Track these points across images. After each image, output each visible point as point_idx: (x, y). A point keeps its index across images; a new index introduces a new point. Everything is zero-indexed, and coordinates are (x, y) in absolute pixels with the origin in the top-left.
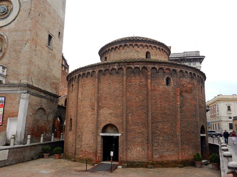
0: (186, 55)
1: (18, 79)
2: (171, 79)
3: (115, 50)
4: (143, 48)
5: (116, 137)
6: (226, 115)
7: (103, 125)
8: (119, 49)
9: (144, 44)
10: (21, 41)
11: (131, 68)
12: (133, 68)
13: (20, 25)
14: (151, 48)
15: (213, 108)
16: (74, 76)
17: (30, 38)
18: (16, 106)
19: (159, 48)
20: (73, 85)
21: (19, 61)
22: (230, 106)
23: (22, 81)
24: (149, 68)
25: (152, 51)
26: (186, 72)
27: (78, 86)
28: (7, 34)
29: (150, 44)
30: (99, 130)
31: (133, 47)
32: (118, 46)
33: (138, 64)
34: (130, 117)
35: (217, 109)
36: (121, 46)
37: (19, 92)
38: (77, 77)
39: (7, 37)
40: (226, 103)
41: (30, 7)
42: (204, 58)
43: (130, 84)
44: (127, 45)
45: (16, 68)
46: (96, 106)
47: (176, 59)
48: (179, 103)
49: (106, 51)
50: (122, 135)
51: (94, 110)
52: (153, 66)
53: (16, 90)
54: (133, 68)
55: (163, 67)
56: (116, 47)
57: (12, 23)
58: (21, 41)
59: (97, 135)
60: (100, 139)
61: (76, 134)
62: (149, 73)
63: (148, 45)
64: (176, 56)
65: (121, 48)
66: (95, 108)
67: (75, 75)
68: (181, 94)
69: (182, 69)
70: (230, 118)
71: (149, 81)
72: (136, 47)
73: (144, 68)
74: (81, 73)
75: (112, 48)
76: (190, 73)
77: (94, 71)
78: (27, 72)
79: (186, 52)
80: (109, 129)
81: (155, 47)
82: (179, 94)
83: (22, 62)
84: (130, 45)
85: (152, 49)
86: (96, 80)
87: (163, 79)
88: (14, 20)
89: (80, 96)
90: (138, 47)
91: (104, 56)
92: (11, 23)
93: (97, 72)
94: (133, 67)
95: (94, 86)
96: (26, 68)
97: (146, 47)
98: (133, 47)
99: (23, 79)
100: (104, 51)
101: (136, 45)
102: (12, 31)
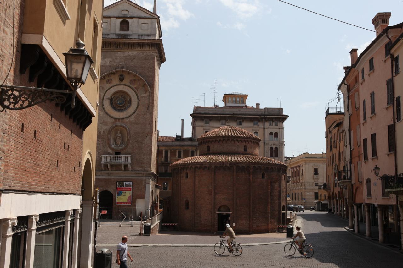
0: (268, 112)
1: (142, 167)
2: (265, 174)
3: (219, 142)
4: (242, 142)
6: (311, 181)
7: (219, 206)
8: (222, 142)
9: (243, 140)
10: (142, 133)
12: (241, 167)
14: (248, 142)
15: (297, 169)
16: (190, 166)
19: (254, 142)
20: (187, 174)
22: (317, 169)
23: (146, 169)
25: (248, 144)
26: (275, 168)
27: (195, 175)
28: (128, 126)
29: (247, 140)
30: (216, 210)
31: (235, 142)
32: (222, 140)
33: (244, 164)
34: (238, 201)
35: (301, 173)
36: (224, 140)
38: (194, 168)
40: (312, 164)
41: (148, 102)
42: (287, 118)
43: (238, 177)
44: (230, 140)
45: (139, 157)
46: (213, 192)
47: (256, 116)
48: (269, 191)
49: (209, 141)
50: (233, 213)
51: (211, 195)
52: (254, 165)
54: (241, 167)
55: (261, 165)
56: (220, 140)
57: (132, 116)
58: (142, 133)
59: (215, 213)
60: (216, 216)
61: (195, 213)
62: (251, 171)
63: (246, 140)
64: (256, 112)
65: (224, 142)
66: (212, 194)
67: (191, 166)
68: (271, 184)
69: (272, 166)
70: (316, 185)
71: (251, 176)
72: (236, 142)
73: (248, 167)
74: (198, 166)
75: (216, 140)
76: (278, 168)
77: (210, 166)
79: (267, 108)
80: (222, 209)
81: (251, 141)
82: (270, 184)
84: (232, 140)
85: (248, 143)
86: (213, 173)
87: (260, 175)
89: (197, 183)
90: (238, 142)
91: (206, 144)
93: (213, 167)
94: (241, 166)
95: (210, 177)
97: (244, 142)
98: (235, 142)
100: (208, 140)
101: (237, 140)
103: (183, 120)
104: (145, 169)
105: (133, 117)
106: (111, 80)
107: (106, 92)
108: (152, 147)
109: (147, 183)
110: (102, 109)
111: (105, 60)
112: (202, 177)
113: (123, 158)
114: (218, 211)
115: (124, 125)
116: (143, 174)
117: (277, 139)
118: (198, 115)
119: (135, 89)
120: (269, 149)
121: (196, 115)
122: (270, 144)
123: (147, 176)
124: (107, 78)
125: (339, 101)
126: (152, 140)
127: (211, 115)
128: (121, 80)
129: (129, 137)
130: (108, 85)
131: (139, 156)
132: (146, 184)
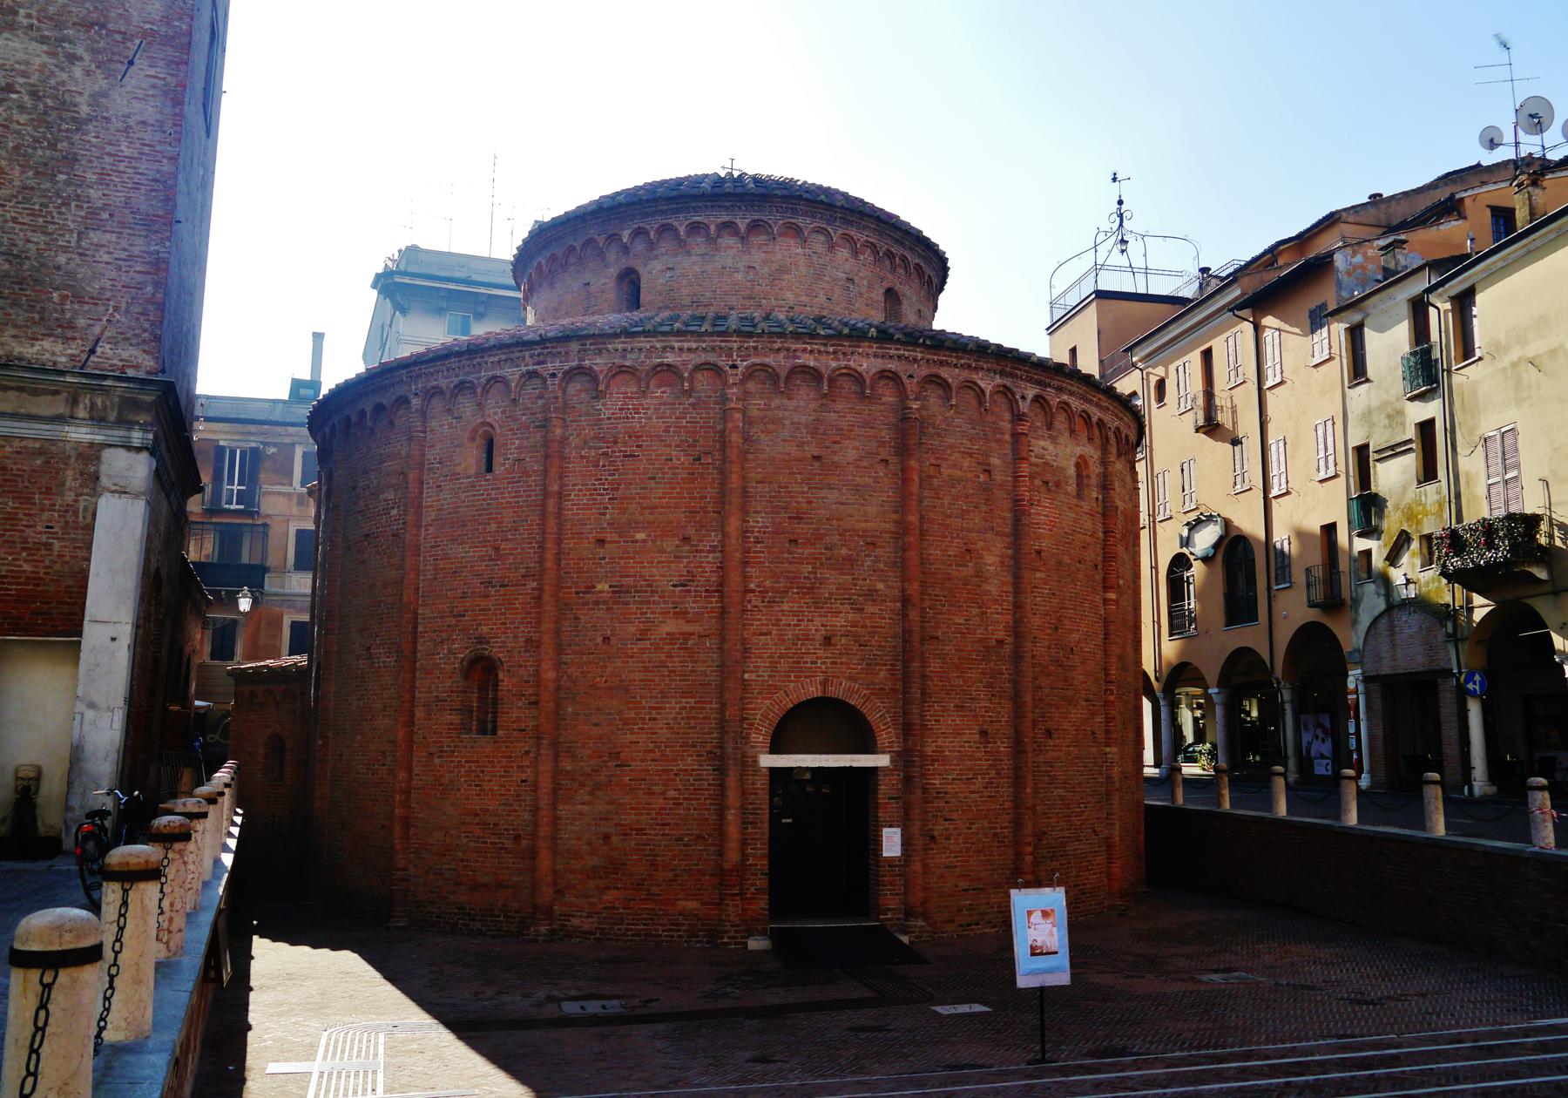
5: (808, 776)
10: (87, 25)
11: (944, 385)
17: (167, 20)
18: (57, 545)
21: (68, 183)
23: (104, 349)
24: (1023, 398)
32: (742, 225)
37: (80, 434)
58: (87, 25)
78: (149, 289)
83: (99, 204)
96: (136, 251)
99: (114, 342)
103: (318, 337)
104: (92, 351)
109: (105, 481)
112: (631, 456)
114: (775, 749)
116: (74, 401)
118: (418, 282)
121: (407, 280)
123: (112, 416)
125: (1123, 251)
127: (483, 290)
132: (95, 494)
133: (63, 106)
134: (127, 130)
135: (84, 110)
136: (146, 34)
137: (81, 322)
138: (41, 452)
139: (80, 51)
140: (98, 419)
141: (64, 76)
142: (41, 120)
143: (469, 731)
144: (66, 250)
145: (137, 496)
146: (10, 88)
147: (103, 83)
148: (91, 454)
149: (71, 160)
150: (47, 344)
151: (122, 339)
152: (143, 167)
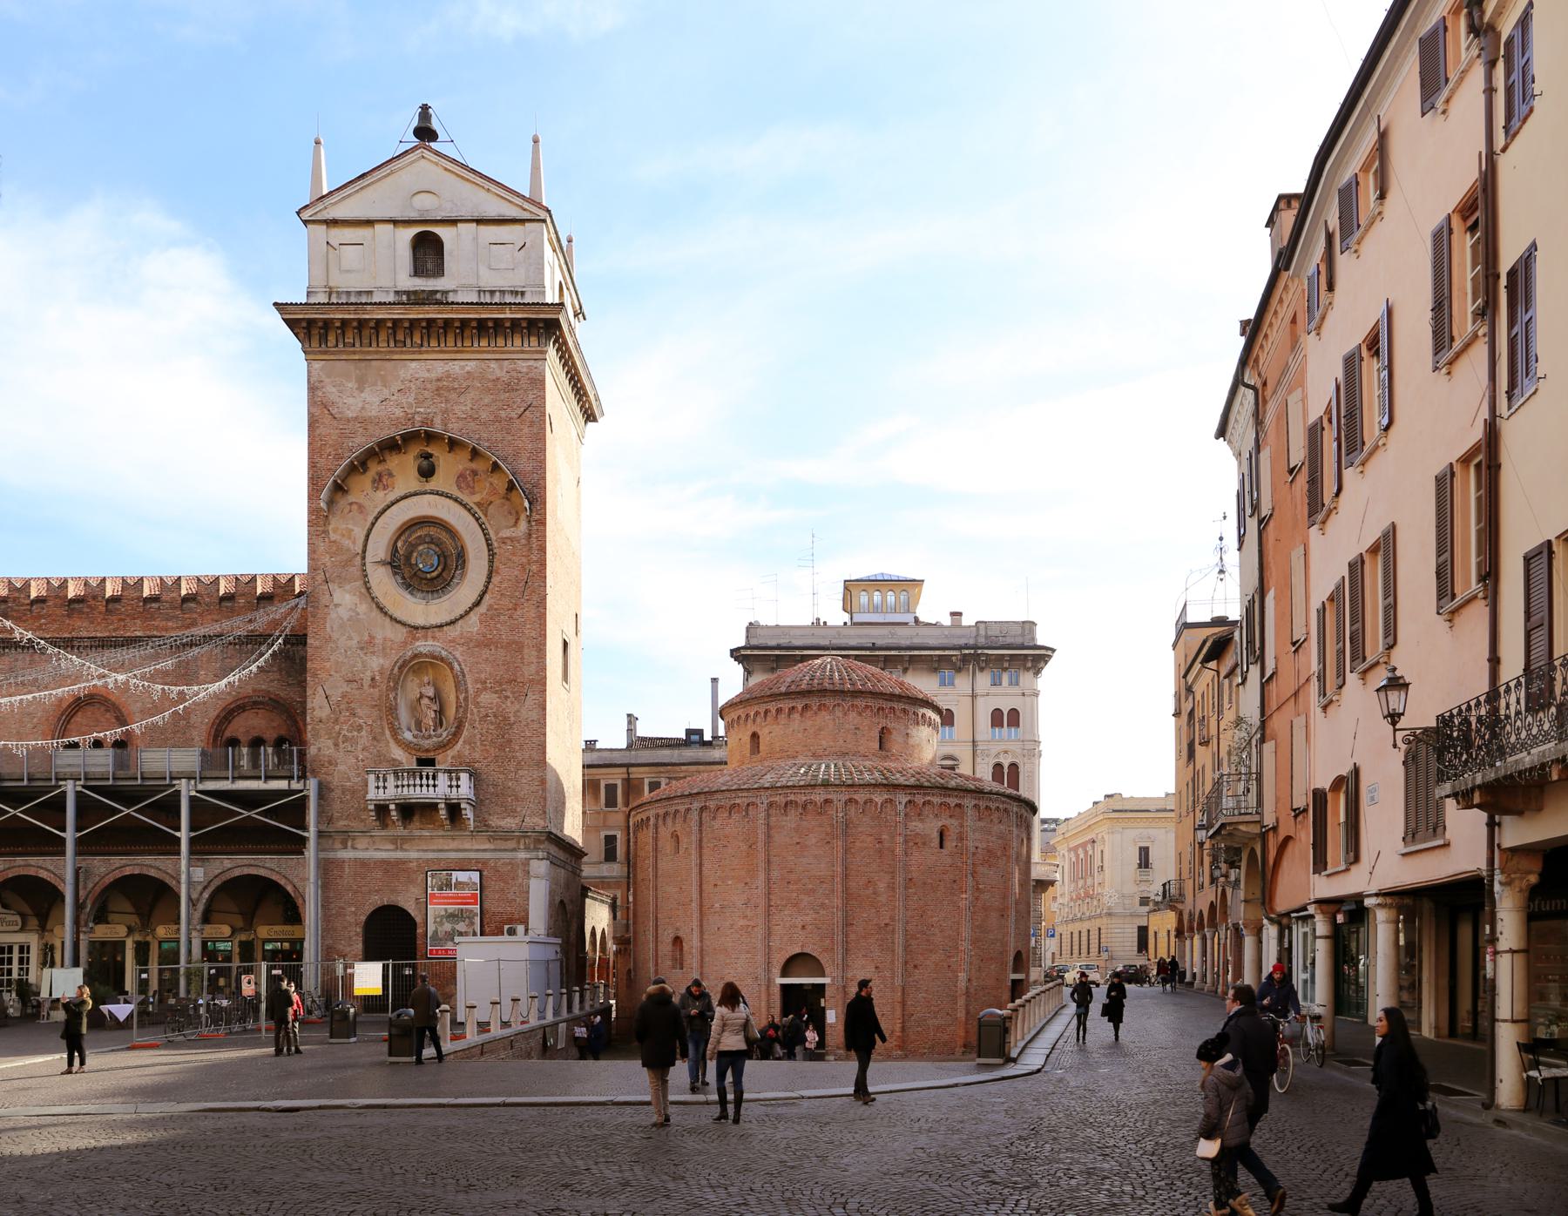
10: (510, 682)
13: (499, 626)
37: (522, 855)
39: (460, 665)
45: (501, 776)
53: (514, 850)
58: (510, 682)
88: (477, 604)
92: (467, 613)
99: (530, 816)
102: (477, 646)
105: (474, 618)
106: (390, 475)
107: (373, 524)
108: (545, 734)
109: (531, 873)
110: (363, 590)
111: (363, 395)
113: (442, 779)
115: (444, 653)
117: (1016, 734)
119: (476, 509)
120: (991, 770)
122: (994, 752)
123: (532, 847)
124: (374, 468)
126: (545, 709)
128: (427, 472)
129: (462, 697)
130: (380, 494)
131: (501, 773)
132: (529, 879)
133: (506, 719)
134: (527, 725)
135: (512, 719)
136: (530, 681)
137: (519, 809)
138: (510, 863)
139: (509, 694)
140: (527, 849)
141: (504, 706)
142: (498, 727)
143: (676, 968)
144: (511, 780)
145: (542, 878)
146: (487, 716)
147: (518, 706)
148: (527, 862)
149: (510, 741)
150: (508, 820)
151: (533, 815)
152: (534, 740)
